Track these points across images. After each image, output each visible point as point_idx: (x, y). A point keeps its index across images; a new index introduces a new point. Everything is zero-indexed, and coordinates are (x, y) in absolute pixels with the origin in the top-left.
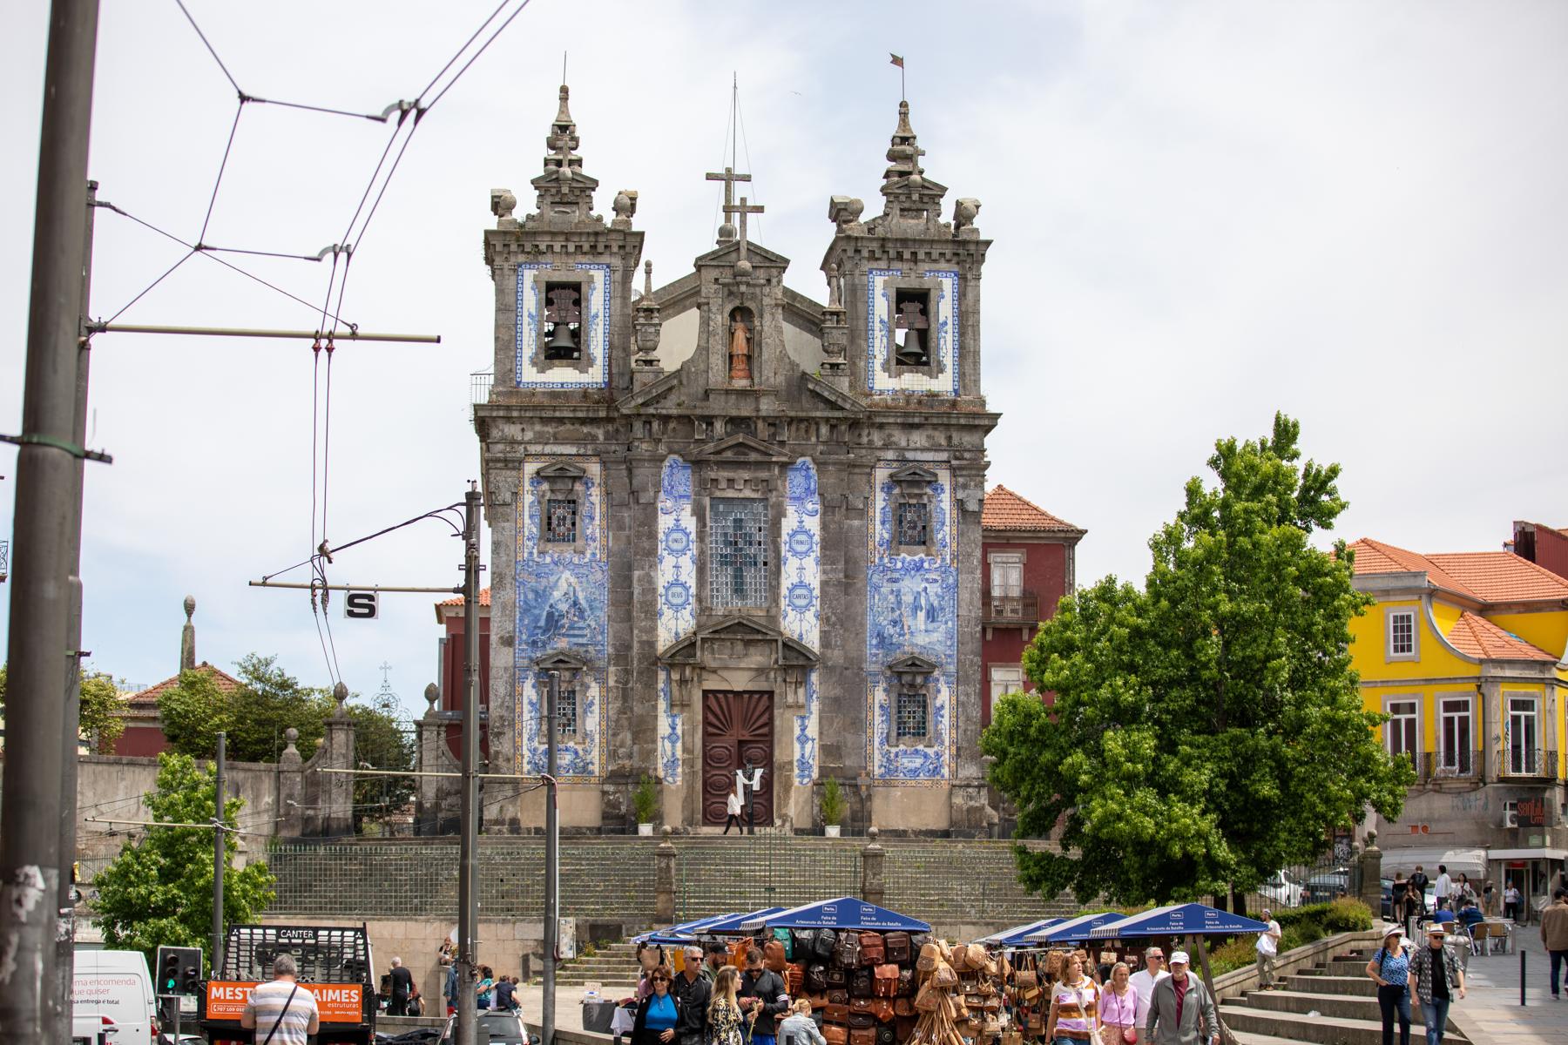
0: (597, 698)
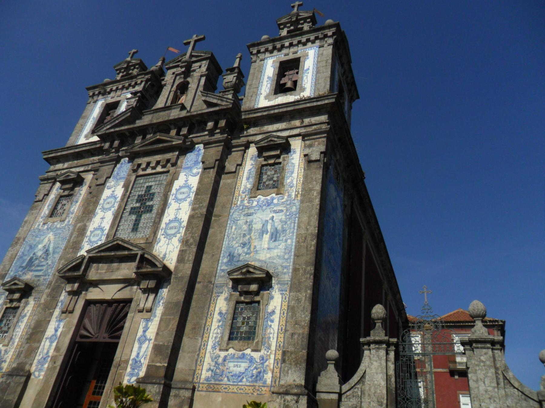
0: (30, 312)
